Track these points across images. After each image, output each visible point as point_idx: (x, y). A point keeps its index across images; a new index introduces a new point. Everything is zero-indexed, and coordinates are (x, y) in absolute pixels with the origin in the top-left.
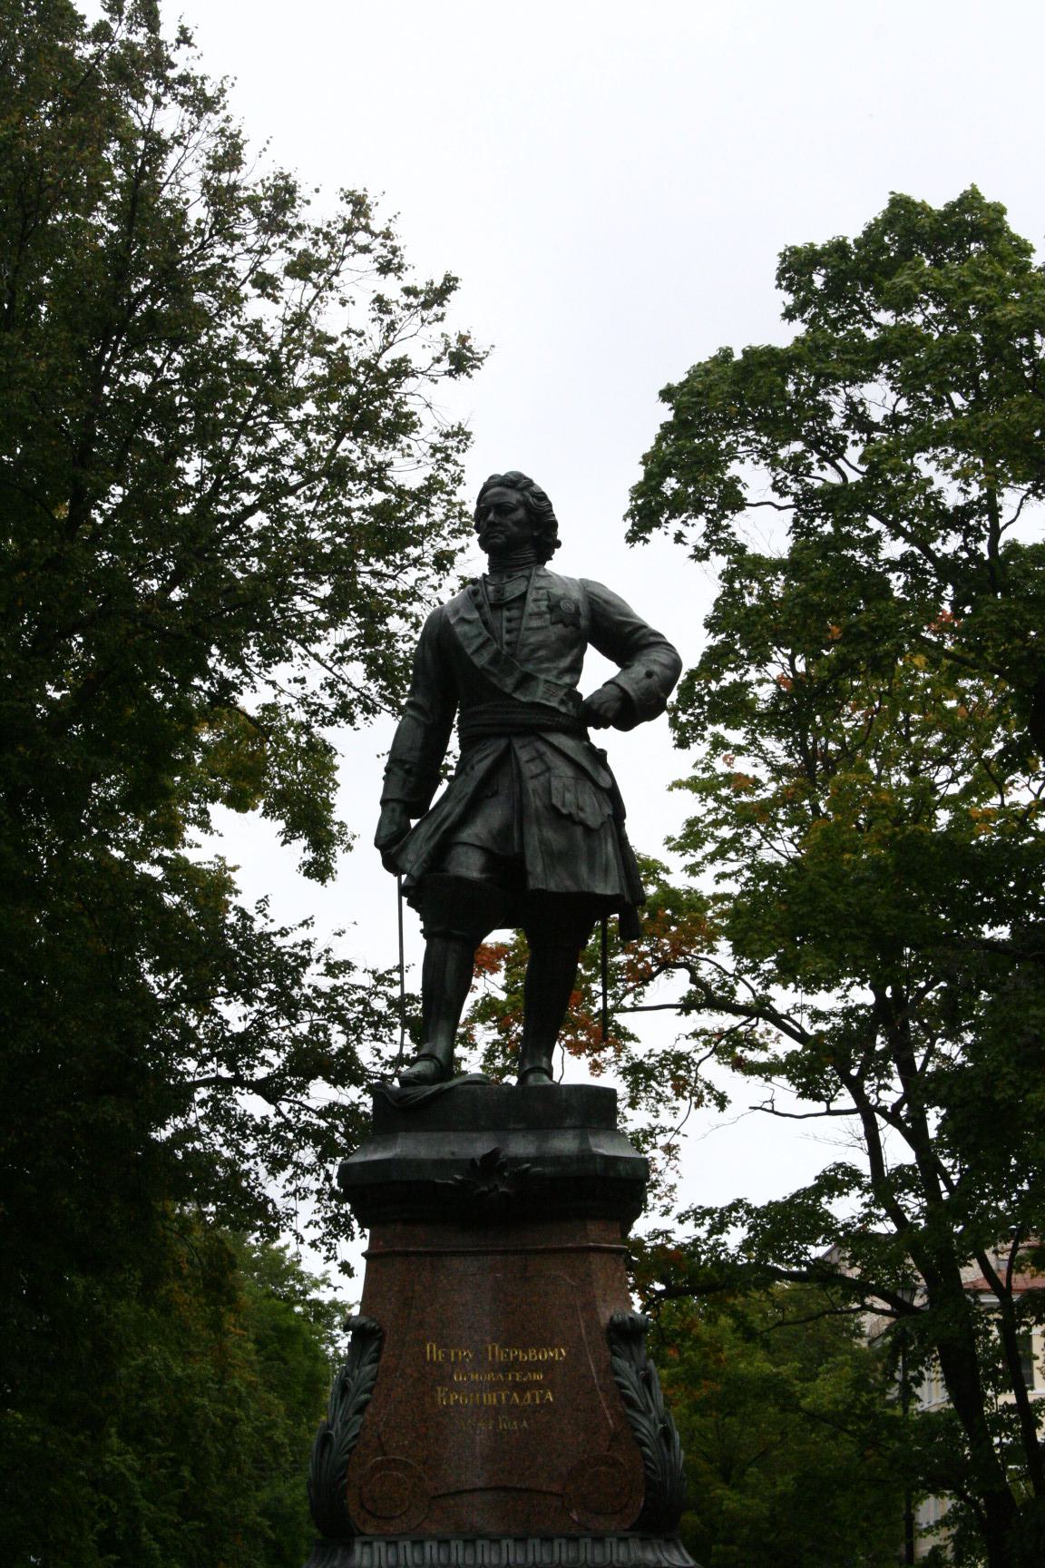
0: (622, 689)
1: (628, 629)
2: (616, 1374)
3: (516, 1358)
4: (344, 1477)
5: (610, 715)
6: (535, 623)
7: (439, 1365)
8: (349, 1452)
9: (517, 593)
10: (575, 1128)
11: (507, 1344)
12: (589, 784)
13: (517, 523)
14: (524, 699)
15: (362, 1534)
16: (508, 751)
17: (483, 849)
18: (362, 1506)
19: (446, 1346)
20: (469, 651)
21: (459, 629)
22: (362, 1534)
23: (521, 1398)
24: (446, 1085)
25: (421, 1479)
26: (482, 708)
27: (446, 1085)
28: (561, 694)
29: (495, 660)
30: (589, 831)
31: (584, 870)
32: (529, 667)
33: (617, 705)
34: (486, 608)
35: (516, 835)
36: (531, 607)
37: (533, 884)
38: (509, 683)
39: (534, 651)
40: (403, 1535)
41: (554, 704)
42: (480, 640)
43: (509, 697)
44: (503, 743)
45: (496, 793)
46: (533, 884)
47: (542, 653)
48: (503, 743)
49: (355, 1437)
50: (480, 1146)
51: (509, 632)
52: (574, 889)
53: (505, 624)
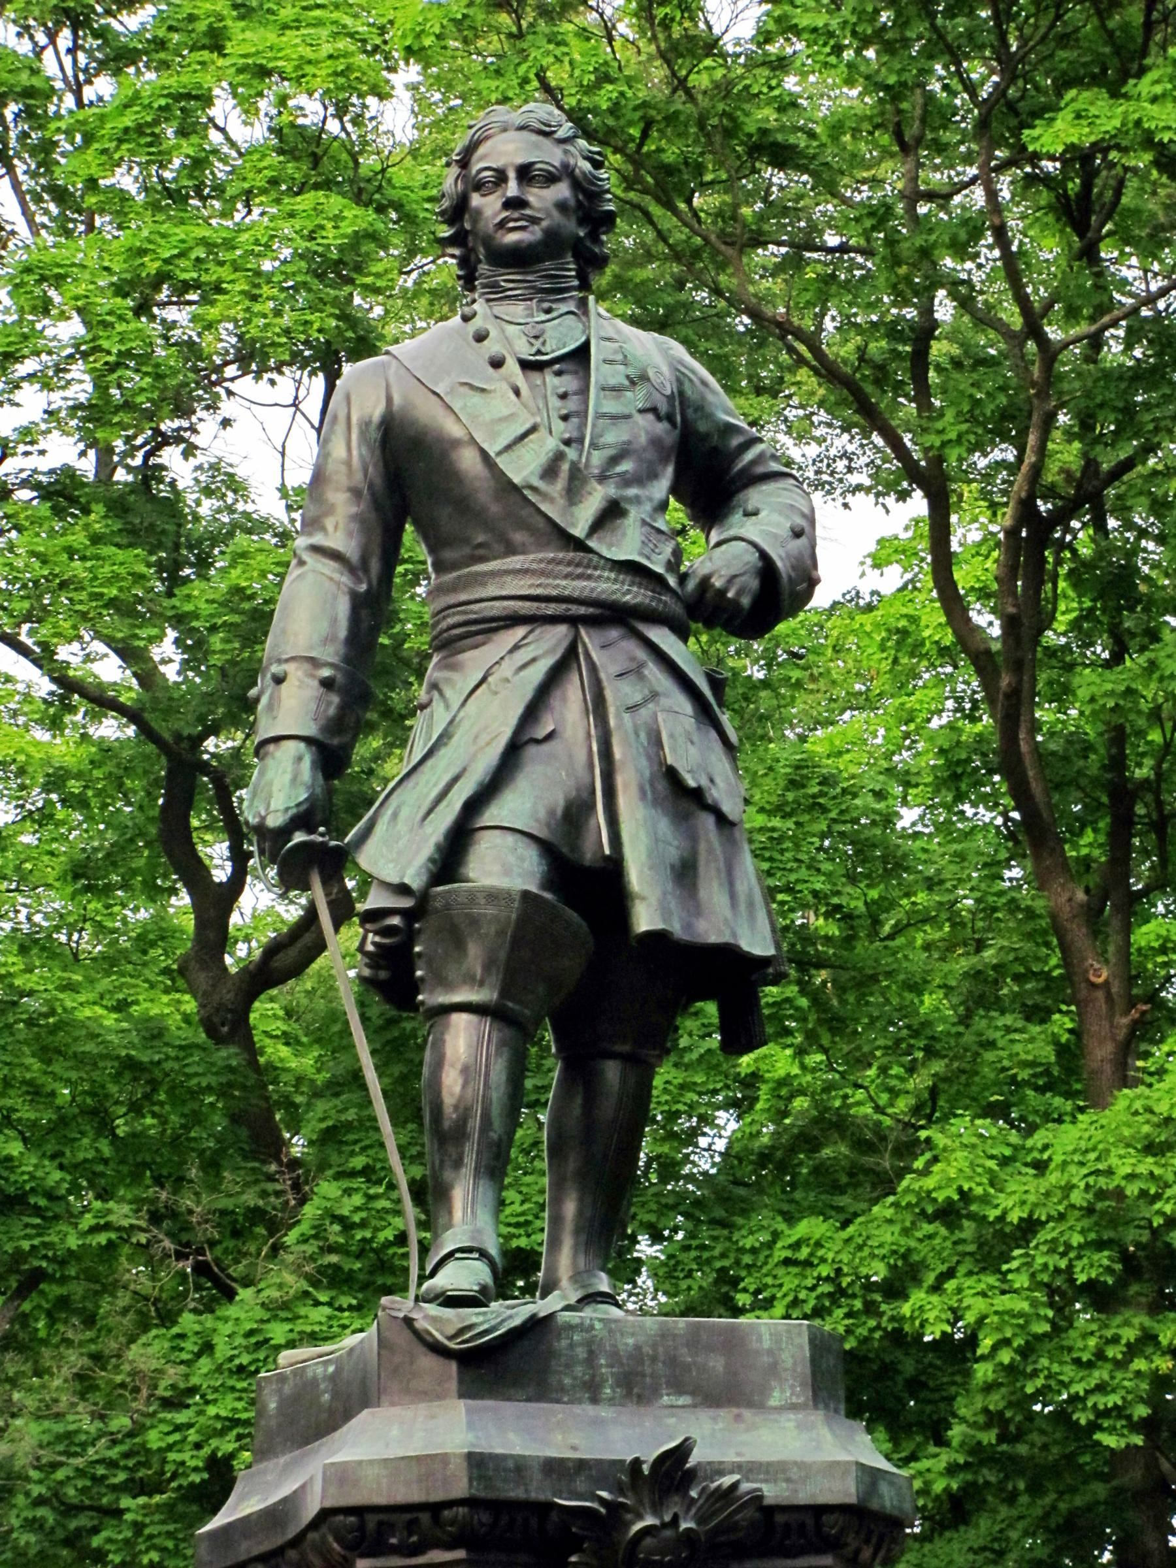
0: (764, 556)
1: (735, 442)
5: (746, 601)
6: (611, 406)
10: (793, 1407)
12: (713, 734)
13: (562, 206)
14: (606, 553)
17: (546, 848)
29: (550, 471)
33: (754, 584)
34: (512, 366)
36: (599, 372)
39: (614, 460)
43: (579, 545)
47: (626, 466)
52: (713, 939)
53: (554, 402)
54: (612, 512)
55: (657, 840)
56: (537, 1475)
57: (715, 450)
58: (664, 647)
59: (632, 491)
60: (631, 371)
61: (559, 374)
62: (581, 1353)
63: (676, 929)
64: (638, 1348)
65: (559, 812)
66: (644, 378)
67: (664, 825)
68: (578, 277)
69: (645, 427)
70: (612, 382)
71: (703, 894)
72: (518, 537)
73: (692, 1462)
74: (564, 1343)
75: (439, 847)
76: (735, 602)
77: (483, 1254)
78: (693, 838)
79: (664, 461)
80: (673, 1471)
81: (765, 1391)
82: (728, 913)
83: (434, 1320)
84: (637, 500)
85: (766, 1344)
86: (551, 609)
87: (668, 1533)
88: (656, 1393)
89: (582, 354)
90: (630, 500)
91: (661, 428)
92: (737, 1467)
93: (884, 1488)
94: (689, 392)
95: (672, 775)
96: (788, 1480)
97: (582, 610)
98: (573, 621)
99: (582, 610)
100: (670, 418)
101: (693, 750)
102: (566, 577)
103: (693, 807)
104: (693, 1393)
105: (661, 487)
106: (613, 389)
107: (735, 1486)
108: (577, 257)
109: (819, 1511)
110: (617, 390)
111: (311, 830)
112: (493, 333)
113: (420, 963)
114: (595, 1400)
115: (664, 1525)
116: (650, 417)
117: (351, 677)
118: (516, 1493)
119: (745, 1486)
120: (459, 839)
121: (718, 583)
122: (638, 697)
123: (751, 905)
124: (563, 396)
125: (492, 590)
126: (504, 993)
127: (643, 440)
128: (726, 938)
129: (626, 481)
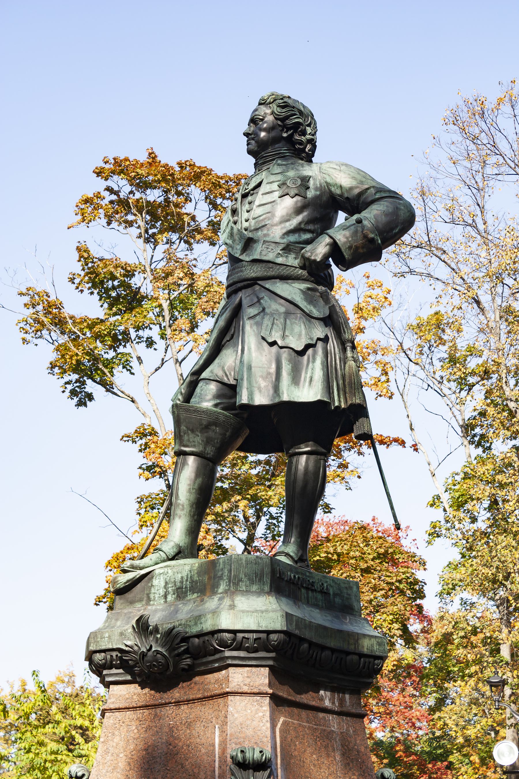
41: (270, 257)
57: (347, 198)
62: (163, 584)
64: (182, 578)
74: (157, 581)
76: (315, 261)
99: (242, 284)
104: (197, 593)
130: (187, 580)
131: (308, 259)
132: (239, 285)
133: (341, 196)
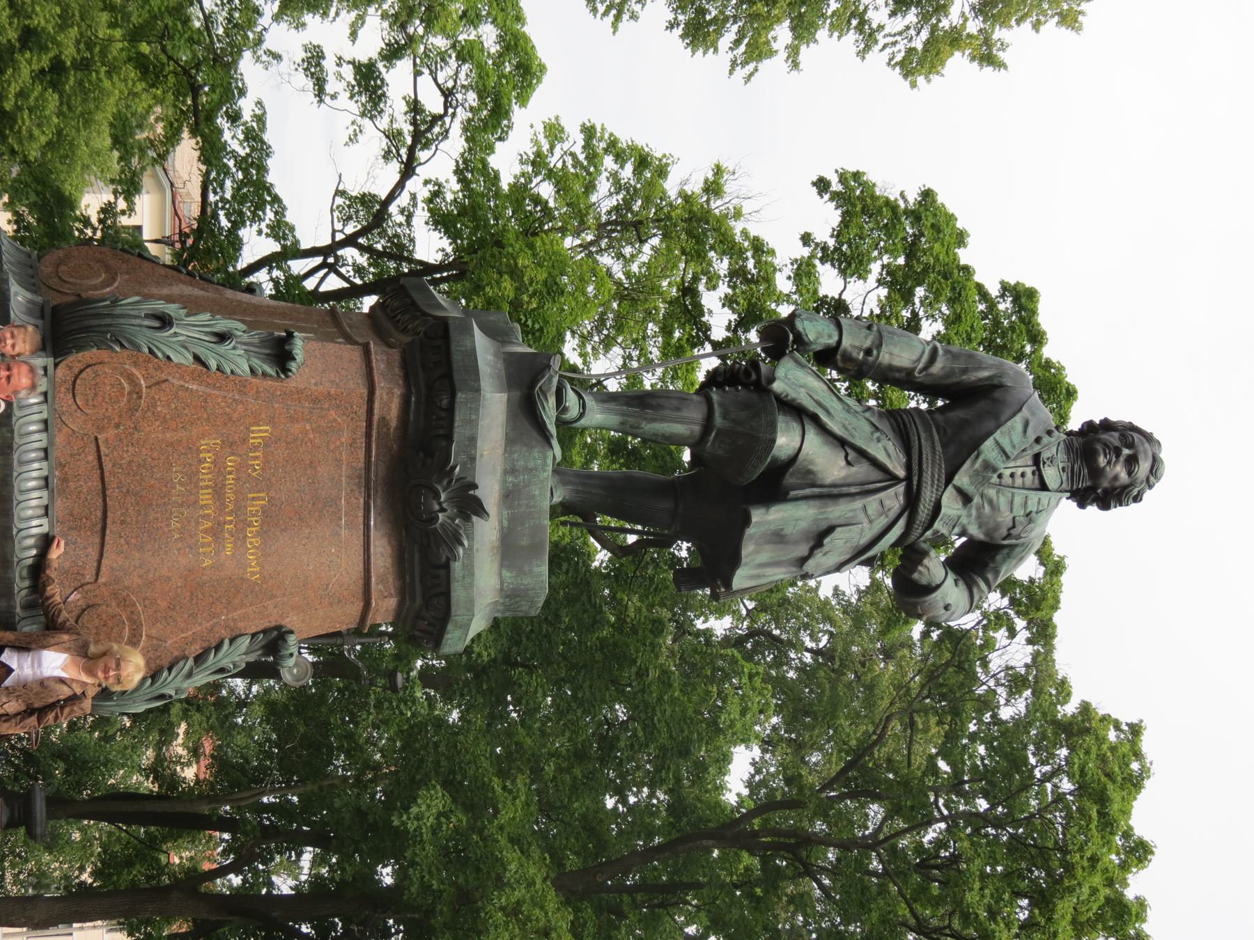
0: (938, 586)
1: (990, 576)
2: (232, 641)
3: (250, 525)
4: (122, 346)
5: (916, 576)
6: (1018, 500)
7: (245, 441)
8: (151, 351)
9: (1047, 481)
10: (502, 583)
11: (265, 512)
12: (848, 557)
13: (1116, 478)
15: (56, 365)
16: (893, 479)
17: (793, 459)
18: (89, 366)
19: (266, 445)
20: (997, 435)
21: (1017, 422)
22: (56, 365)
23: (206, 531)
24: (555, 442)
25: (117, 426)
26: (939, 448)
27: (555, 442)
28: (944, 531)
29: (989, 467)
30: (803, 561)
31: (764, 557)
32: (977, 500)
33: (924, 581)
34: (1037, 448)
35: (807, 491)
36: (1034, 496)
37: (757, 515)
38: (962, 479)
39: (991, 502)
40: (53, 410)
42: (1008, 449)
43: (949, 480)
44: (901, 473)
45: (849, 463)
46: (757, 515)
47: (987, 508)
48: (901, 473)
49: (169, 358)
50: (489, 490)
51: (1012, 475)
52: (744, 553)
53: (1020, 470)
54: (966, 499)
55: (797, 520)
56: (467, 433)
58: (887, 537)
59: (974, 512)
60: (1033, 515)
61: (1033, 473)
62: (531, 464)
63: (750, 531)
65: (811, 467)
66: (1030, 521)
67: (803, 525)
68: (1078, 489)
69: (1005, 518)
70: (1029, 502)
71: (767, 547)
72: (952, 449)
73: (475, 518)
75: (794, 400)
76: (914, 570)
77: (582, 415)
78: (796, 542)
79: (987, 534)
80: (471, 506)
81: (510, 568)
82: (757, 561)
83: (550, 380)
84: (969, 515)
85: (536, 569)
86: (915, 467)
87: (437, 507)
88: (509, 507)
89: (1043, 487)
90: (970, 511)
91: (1004, 532)
92: (471, 548)
93: (457, 633)
94: (1018, 550)
95: (830, 529)
96: (464, 577)
97: (915, 483)
98: (908, 478)
99: (915, 483)
100: (1008, 536)
101: (842, 542)
102: (933, 474)
103: (812, 543)
104: (509, 528)
105: (974, 531)
106: (1026, 502)
107: (462, 544)
108: (1088, 489)
109: (447, 595)
110: (1025, 505)
111: (794, 342)
112: (1052, 440)
113: (733, 389)
114: (506, 472)
115: (440, 504)
116: (1011, 524)
117: (871, 366)
118: (459, 417)
119: (461, 551)
120: (799, 413)
121: (926, 561)
122: (870, 512)
123: (759, 576)
124: (1023, 475)
125: (923, 435)
126: (719, 432)
127: (1000, 519)
128: (744, 561)
129: (980, 509)
130: (528, 506)
131: (920, 562)
132: (915, 479)
133: (993, 559)
